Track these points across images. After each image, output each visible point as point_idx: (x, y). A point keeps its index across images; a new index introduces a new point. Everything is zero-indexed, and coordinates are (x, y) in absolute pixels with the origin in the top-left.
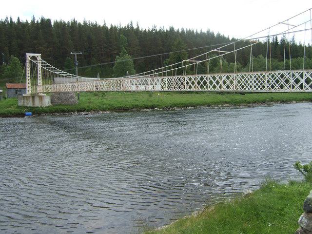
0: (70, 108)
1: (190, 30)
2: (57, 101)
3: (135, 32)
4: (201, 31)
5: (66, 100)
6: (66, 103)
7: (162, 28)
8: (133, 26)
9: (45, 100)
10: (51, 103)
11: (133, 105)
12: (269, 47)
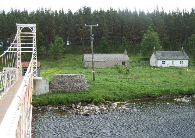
0: (72, 97)
1: (16, 11)
2: (58, 86)
3: (73, 16)
4: (119, 10)
5: (70, 85)
6: (69, 88)
7: (61, 10)
8: (159, 10)
9: (40, 85)
10: (50, 88)
11: (162, 91)
12: (4, 64)
